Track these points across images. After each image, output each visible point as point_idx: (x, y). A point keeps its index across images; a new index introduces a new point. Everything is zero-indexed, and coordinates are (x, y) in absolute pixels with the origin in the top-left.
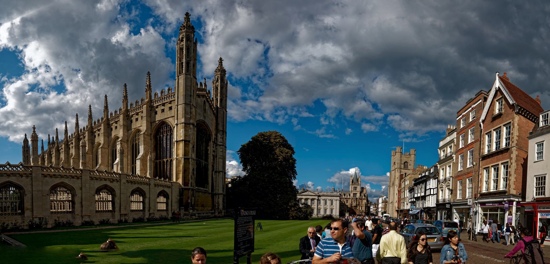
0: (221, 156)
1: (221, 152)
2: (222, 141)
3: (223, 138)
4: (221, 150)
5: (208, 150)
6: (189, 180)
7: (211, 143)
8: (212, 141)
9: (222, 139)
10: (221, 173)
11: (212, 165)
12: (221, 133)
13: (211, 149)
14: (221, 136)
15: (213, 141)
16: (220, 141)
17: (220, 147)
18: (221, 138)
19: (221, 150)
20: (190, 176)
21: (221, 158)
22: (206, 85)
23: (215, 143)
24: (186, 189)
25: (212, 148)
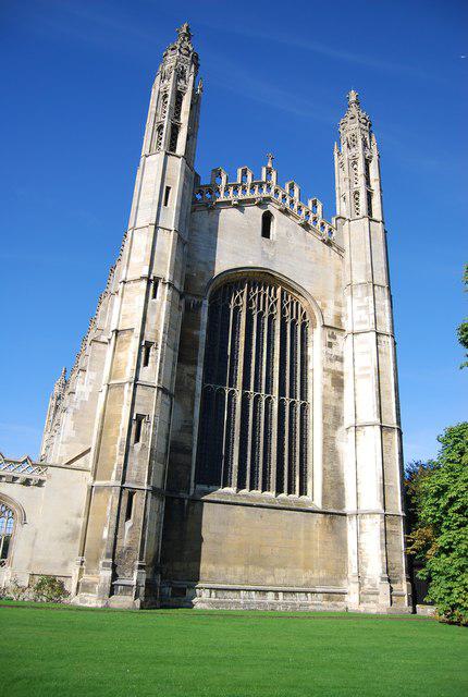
0: (369, 368)
2: (366, 318)
6: (114, 458)
7: (316, 338)
11: (325, 407)
12: (359, 292)
14: (361, 299)
15: (324, 326)
18: (360, 308)
20: (118, 446)
21: (368, 375)
23: (335, 330)
24: (100, 489)
25: (325, 349)
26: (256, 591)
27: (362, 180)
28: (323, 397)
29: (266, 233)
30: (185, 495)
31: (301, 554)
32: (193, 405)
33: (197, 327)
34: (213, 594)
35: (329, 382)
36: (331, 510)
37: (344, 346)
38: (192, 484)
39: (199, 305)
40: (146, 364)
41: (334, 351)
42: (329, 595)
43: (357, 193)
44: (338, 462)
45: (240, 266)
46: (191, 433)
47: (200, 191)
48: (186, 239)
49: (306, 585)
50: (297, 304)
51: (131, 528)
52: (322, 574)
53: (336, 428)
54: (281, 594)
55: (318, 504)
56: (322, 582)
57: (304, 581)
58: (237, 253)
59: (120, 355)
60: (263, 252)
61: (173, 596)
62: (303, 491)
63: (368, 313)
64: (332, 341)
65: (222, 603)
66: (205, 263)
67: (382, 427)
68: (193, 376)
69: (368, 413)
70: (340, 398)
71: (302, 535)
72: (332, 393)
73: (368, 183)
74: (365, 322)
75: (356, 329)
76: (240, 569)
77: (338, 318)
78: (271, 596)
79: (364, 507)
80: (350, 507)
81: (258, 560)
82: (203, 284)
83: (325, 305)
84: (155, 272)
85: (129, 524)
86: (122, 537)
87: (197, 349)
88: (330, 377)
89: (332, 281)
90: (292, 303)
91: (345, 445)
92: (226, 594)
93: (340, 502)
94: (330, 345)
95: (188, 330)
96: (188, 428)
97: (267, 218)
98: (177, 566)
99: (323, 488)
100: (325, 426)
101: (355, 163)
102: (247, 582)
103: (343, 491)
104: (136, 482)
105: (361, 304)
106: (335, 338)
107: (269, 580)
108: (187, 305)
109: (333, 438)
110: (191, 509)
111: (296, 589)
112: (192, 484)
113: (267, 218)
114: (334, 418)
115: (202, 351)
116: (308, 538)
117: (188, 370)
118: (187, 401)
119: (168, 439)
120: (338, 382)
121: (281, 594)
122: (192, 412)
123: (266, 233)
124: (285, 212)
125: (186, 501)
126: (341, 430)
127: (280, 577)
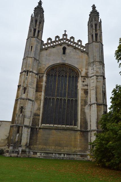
1: (92, 83)
3: (94, 68)
4: (92, 81)
5: (76, 87)
7: (80, 80)
8: (80, 77)
9: (93, 70)
10: (93, 105)
11: (82, 100)
13: (80, 85)
16: (91, 73)
17: (91, 78)
18: (92, 69)
19: (92, 81)
22: (65, 35)
25: (82, 83)
26: (58, 154)
27: (94, 31)
28: (81, 97)
29: (64, 53)
30: (37, 127)
31: (73, 143)
32: (40, 103)
33: (42, 81)
34: (45, 154)
35: (83, 92)
36: (83, 130)
37: (87, 81)
38: (40, 124)
39: (43, 76)
40: (24, 93)
41: (85, 83)
42: (82, 156)
43: (92, 35)
44: (85, 116)
45: (55, 63)
46: (40, 110)
47: (44, 45)
48: (38, 59)
49: (74, 152)
50: (74, 71)
51: (18, 136)
52: (80, 149)
53: (85, 106)
54: (66, 155)
55: (79, 128)
56: (80, 151)
57: (74, 151)
58: (54, 60)
59: (19, 92)
60: (62, 58)
61: (33, 154)
62: (75, 125)
63: (94, 70)
64: (84, 80)
65: (47, 157)
66: (45, 64)
67: (97, 104)
68: (41, 95)
69: (93, 101)
70: (87, 97)
71: (73, 137)
72: (84, 95)
73: (96, 31)
74: (93, 73)
75: (91, 75)
76: (53, 147)
77: (87, 73)
78: (62, 156)
79: (92, 129)
80: (89, 129)
81: (59, 145)
82: (44, 70)
83: (82, 70)
84: (28, 69)
86: (16, 138)
87: (42, 88)
88: (83, 91)
89: (85, 63)
90: (72, 71)
91: (87, 111)
92: (49, 154)
93: (86, 127)
94: (83, 82)
95: (39, 83)
96: (39, 109)
97: (64, 49)
98: (35, 146)
99: (81, 123)
100: (82, 105)
101: (92, 26)
102: (55, 151)
103: (87, 124)
104: (20, 124)
105: (92, 68)
106: (85, 79)
107: (62, 151)
109: (84, 109)
110: (39, 131)
111: (70, 153)
112: (40, 124)
113: (64, 49)
114: (85, 103)
115: (43, 88)
116: (75, 138)
117: (39, 93)
118: (39, 102)
119: (31, 112)
120: (86, 92)
121: (66, 155)
122: (40, 105)
123: (64, 53)
125: (38, 129)
126: (87, 106)
127: (66, 150)
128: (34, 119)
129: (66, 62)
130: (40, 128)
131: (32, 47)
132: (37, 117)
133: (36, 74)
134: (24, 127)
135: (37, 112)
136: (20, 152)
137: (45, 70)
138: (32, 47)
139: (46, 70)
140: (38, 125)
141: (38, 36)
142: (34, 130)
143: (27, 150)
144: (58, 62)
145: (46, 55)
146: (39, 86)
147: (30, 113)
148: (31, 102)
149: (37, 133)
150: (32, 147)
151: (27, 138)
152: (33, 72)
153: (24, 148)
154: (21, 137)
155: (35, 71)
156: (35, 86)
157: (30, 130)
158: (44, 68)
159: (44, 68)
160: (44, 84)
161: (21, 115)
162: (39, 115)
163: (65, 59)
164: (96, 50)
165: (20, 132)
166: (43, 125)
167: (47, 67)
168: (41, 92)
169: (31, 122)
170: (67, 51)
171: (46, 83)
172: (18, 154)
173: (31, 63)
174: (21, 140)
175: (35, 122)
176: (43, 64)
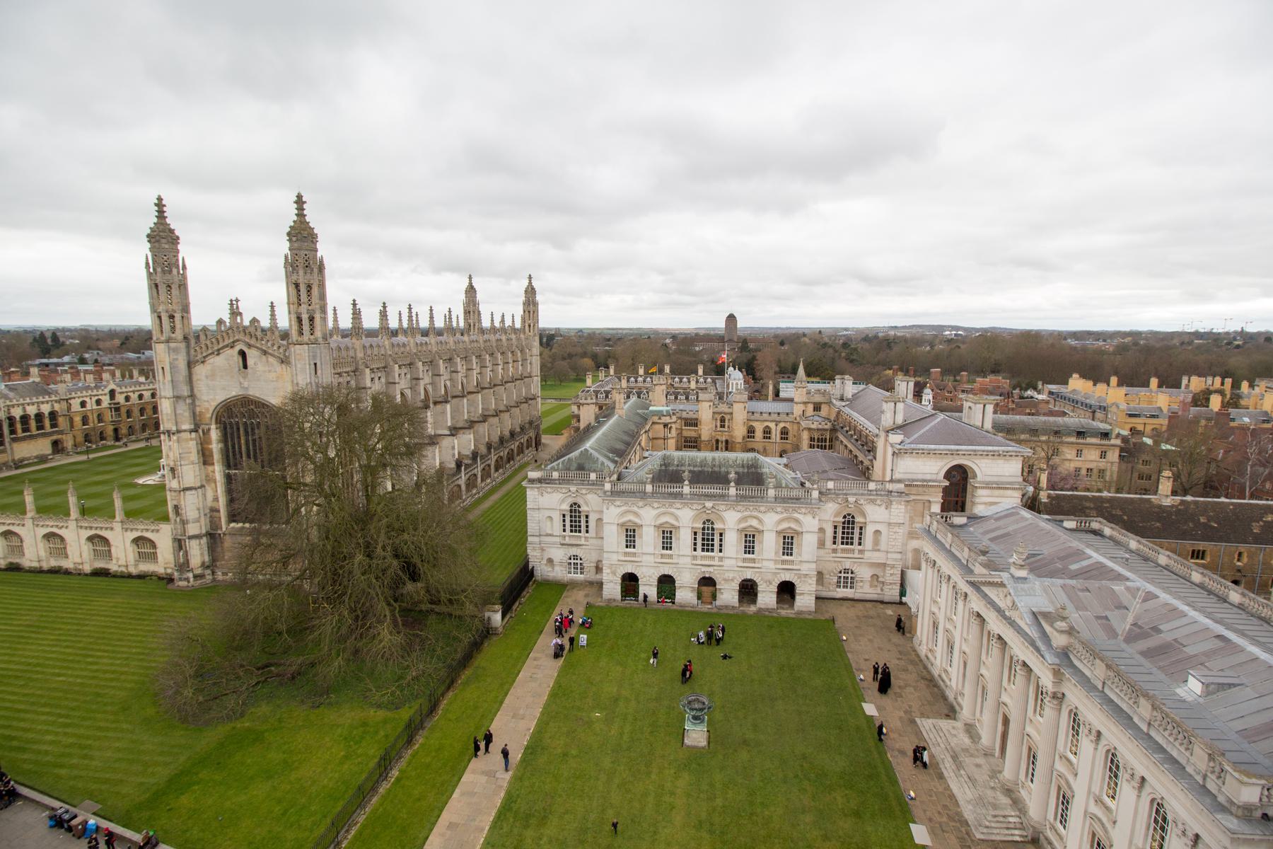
30: (219, 532)
33: (210, 442)
39: (209, 430)
45: (228, 397)
46: (218, 501)
60: (241, 383)
68: (214, 472)
82: (209, 415)
85: (181, 554)
95: (205, 446)
96: (216, 499)
97: (243, 354)
108: (203, 431)
113: (243, 354)
115: (217, 456)
117: (210, 468)
118: (213, 485)
119: (199, 509)
122: (217, 491)
124: (250, 346)
128: (211, 517)
129: (251, 393)
130: (224, 534)
131: (163, 368)
132: (215, 514)
133: (191, 431)
134: (187, 540)
135: (215, 505)
136: (192, 580)
137: (210, 415)
138: (163, 368)
139: (212, 414)
140: (221, 528)
141: (173, 329)
142: (213, 538)
143: (208, 572)
144: (234, 394)
145: (207, 377)
146: (207, 453)
147: (197, 512)
148: (193, 492)
149: (222, 543)
150: (218, 563)
151: (202, 554)
152: (179, 431)
153: (199, 571)
154: (187, 555)
155: (185, 427)
156: (194, 456)
157: (204, 540)
158: (208, 409)
159: (208, 409)
160: (216, 447)
161: (178, 519)
162: (219, 511)
163: (246, 384)
164: (299, 366)
165: (184, 547)
166: (232, 525)
167: (213, 408)
168: (213, 464)
169: (203, 528)
170: (250, 362)
171: (220, 441)
172: (189, 582)
173: (169, 412)
174: (188, 560)
175: (214, 523)
176: (205, 401)
